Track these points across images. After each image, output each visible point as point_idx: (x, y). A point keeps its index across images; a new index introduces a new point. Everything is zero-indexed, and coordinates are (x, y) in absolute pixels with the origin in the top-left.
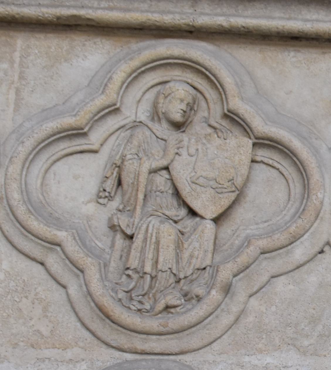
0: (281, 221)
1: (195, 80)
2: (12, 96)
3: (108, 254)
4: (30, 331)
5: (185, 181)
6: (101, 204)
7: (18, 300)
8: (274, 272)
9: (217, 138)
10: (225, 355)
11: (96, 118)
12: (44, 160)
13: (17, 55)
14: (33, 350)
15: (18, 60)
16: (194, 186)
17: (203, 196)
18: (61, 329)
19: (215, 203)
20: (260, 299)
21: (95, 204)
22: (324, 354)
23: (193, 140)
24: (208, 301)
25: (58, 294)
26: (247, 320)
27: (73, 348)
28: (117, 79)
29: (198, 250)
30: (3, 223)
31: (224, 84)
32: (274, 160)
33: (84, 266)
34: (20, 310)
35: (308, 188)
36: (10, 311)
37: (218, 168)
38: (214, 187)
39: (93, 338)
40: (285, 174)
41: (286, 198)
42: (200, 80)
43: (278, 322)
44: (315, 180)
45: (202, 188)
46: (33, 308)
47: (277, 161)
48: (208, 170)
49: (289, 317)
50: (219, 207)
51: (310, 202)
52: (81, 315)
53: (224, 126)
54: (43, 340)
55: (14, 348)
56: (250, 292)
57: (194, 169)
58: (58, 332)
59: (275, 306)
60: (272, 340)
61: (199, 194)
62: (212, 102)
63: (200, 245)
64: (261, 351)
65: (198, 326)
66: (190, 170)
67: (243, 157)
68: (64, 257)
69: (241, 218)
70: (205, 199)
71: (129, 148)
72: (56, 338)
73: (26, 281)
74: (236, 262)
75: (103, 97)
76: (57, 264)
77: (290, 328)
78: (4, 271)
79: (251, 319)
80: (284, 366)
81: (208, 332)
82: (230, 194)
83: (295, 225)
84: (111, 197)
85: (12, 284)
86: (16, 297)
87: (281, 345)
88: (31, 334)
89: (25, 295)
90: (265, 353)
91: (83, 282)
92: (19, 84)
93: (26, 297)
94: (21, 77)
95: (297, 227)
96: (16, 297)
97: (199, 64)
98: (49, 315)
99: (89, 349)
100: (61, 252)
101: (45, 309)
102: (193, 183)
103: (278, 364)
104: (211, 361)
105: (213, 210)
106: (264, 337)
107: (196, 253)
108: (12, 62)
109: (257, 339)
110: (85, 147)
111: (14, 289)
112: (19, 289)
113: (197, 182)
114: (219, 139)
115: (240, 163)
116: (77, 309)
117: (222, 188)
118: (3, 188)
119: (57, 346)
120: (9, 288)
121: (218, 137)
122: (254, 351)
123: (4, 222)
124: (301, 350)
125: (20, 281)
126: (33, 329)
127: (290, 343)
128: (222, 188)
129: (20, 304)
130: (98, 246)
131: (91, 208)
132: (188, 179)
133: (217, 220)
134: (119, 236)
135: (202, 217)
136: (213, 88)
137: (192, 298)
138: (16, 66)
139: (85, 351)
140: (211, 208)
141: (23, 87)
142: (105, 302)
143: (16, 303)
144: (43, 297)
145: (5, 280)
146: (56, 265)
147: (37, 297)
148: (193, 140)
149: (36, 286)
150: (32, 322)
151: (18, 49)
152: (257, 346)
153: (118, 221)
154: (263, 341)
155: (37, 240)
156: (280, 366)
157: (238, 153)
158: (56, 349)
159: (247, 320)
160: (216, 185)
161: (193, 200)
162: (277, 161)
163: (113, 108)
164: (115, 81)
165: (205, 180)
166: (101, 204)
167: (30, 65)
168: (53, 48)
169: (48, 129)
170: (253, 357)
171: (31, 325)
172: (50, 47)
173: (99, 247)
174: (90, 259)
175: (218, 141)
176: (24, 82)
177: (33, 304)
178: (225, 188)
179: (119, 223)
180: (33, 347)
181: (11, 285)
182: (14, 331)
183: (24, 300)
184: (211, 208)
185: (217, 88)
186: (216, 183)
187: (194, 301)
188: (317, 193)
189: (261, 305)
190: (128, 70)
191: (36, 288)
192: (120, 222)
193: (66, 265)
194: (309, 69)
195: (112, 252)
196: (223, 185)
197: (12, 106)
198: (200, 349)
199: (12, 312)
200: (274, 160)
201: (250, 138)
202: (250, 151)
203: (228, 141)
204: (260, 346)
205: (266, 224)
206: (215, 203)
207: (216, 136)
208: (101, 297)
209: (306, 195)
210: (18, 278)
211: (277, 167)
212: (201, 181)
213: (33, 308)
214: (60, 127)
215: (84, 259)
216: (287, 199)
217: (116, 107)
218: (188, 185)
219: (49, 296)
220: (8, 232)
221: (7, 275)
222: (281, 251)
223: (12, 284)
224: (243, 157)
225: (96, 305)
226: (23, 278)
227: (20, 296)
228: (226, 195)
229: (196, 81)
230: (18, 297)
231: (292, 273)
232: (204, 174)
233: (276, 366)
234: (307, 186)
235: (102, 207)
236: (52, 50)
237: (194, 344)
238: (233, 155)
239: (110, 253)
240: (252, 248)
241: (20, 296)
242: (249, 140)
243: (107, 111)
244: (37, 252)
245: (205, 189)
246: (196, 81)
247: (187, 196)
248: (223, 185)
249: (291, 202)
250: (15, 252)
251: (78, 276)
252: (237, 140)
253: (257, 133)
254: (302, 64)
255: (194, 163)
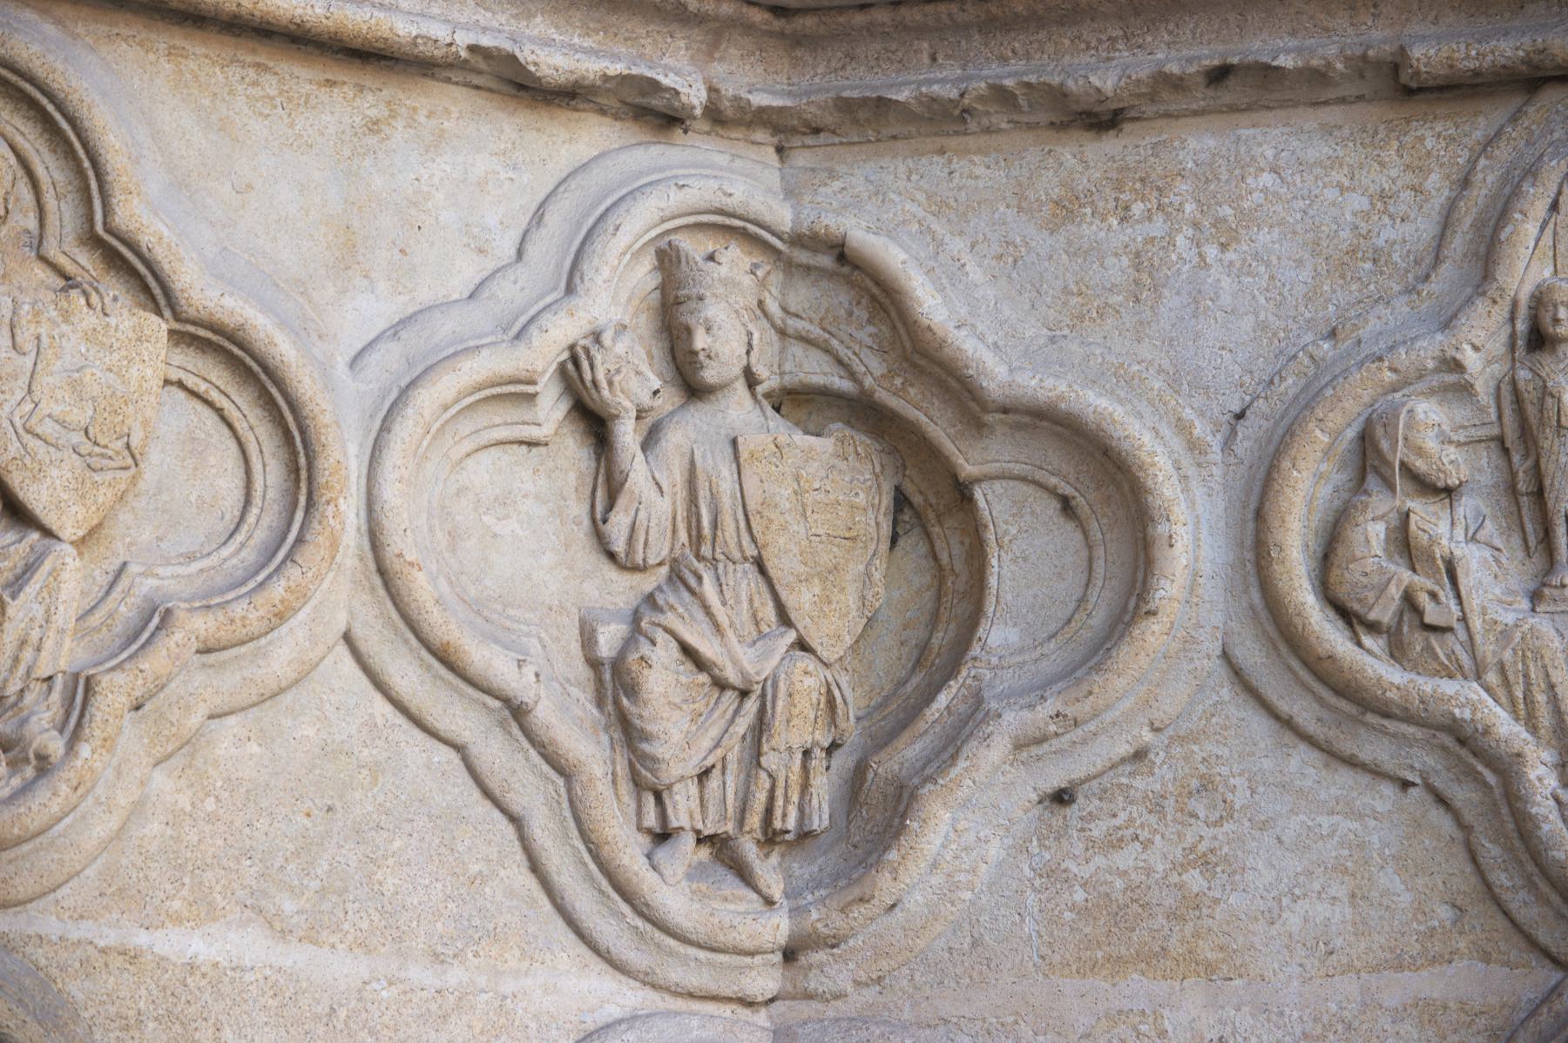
0: (234, 561)
1: (7, 118)
5: (6, 424)
8: (218, 702)
9: (85, 309)
10: (91, 922)
16: (27, 438)
17: (55, 472)
19: (83, 496)
20: (176, 774)
22: (331, 940)
23: (26, 307)
24: (72, 774)
26: (146, 831)
29: (41, 626)
31: (102, 151)
32: (211, 383)
35: (310, 479)
37: (93, 399)
38: (83, 452)
40: (237, 425)
41: (237, 495)
42: (18, 121)
43: (220, 842)
44: (331, 460)
45: (52, 450)
47: (217, 387)
48: (67, 399)
49: (247, 831)
50: (94, 508)
51: (320, 523)
53: (83, 268)
56: (158, 752)
57: (30, 391)
59: (212, 799)
60: (206, 890)
61: (44, 468)
62: (51, 190)
63: (47, 611)
64: (178, 920)
65: (38, 840)
66: (19, 395)
67: (149, 372)
69: (128, 540)
70: (58, 482)
74: (141, 671)
77: (248, 862)
79: (154, 827)
80: (233, 965)
81: (56, 856)
82: (119, 474)
83: (283, 582)
87: (228, 908)
90: (188, 925)
95: (288, 589)
97: (32, 80)
102: (28, 432)
103: (221, 959)
104: (53, 937)
105: (80, 517)
106: (187, 880)
107: (35, 635)
109: (168, 887)
113: (39, 430)
114: (91, 312)
115: (141, 386)
117: (102, 455)
121: (89, 304)
122: (161, 918)
124: (278, 926)
127: (248, 903)
128: (102, 455)
132: (18, 422)
133: (81, 543)
135: (47, 533)
136: (54, 151)
137: (27, 761)
140: (74, 509)
148: (26, 307)
152: (168, 903)
154: (184, 892)
156: (225, 964)
157: (137, 359)
159: (146, 831)
160: (87, 447)
161: (27, 481)
162: (217, 387)
165: (58, 427)
170: (160, 933)
175: (90, 320)
178: (110, 458)
184: (74, 509)
185: (70, 152)
186: (84, 439)
187: (29, 772)
188: (337, 499)
189: (178, 791)
194: (291, 125)
196: (105, 447)
198: (31, 900)
200: (211, 383)
201: (159, 313)
202: (163, 352)
203: (113, 321)
204: (176, 904)
205: (195, 567)
206: (83, 496)
207: (82, 301)
209: (302, 499)
211: (218, 405)
212: (48, 428)
216: (242, 500)
218: (14, 438)
222: (243, 649)
224: (149, 372)
228: (109, 476)
229: (7, 122)
231: (255, 709)
232: (57, 410)
233: (216, 965)
234: (304, 474)
237: (21, 889)
238: (125, 363)
240: (178, 636)
242: (160, 320)
245: (59, 455)
246: (7, 122)
247: (10, 468)
248: (105, 447)
249: (255, 511)
252: (135, 319)
253: (185, 308)
254: (275, 107)
255: (28, 374)
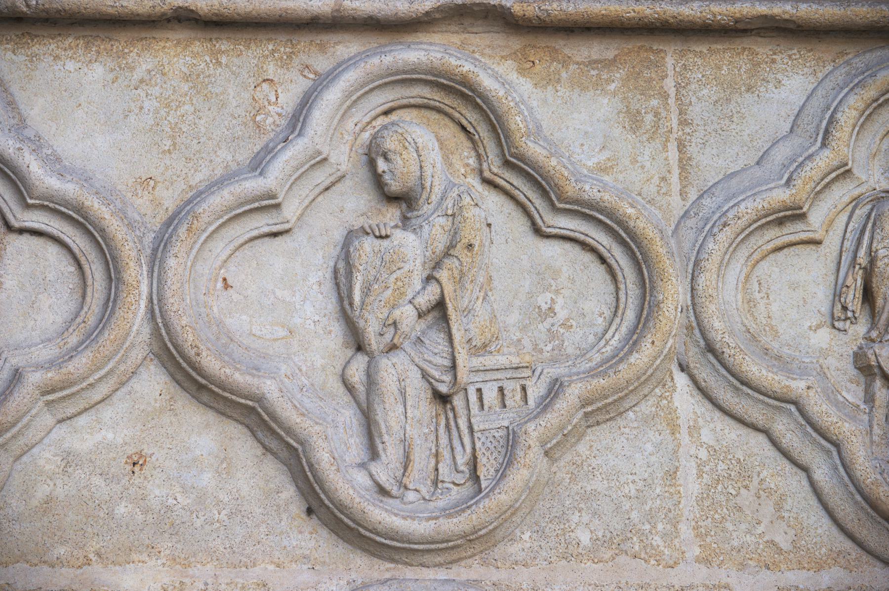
2: (673, 154)
3: (865, 413)
4: (761, 541)
6: (839, 330)
7: (734, 493)
11: (818, 188)
12: (742, 261)
13: (669, 84)
14: (768, 572)
15: (672, 92)
18: (807, 539)
21: (828, 330)
25: (796, 482)
27: (830, 568)
28: (845, 122)
30: (696, 367)
33: (841, 437)
34: (740, 509)
36: (725, 510)
39: (859, 550)
46: (760, 504)
52: (840, 515)
54: (782, 557)
55: (739, 570)
58: (803, 542)
68: (803, 423)
71: (879, 237)
72: (802, 553)
73: (742, 460)
75: (826, 152)
76: (791, 432)
78: (705, 446)
84: (856, 318)
85: (722, 466)
86: (730, 487)
88: (761, 546)
89: (744, 484)
91: (838, 462)
92: (680, 133)
93: (746, 487)
94: (684, 123)
96: (730, 487)
98: (786, 515)
99: (856, 570)
100: (797, 413)
101: (779, 507)
108: (665, 96)
110: (804, 236)
111: (726, 475)
112: (733, 474)
116: (831, 504)
118: (692, 311)
119: (806, 565)
120: (717, 473)
123: (698, 365)
125: (733, 462)
126: (765, 539)
129: (738, 498)
130: (847, 400)
131: (823, 337)
134: (878, 383)
138: (672, 101)
139: (851, 572)
141: (688, 137)
142: (882, 494)
143: (731, 497)
144: (772, 486)
145: (709, 460)
146: (788, 435)
147: (763, 487)
149: (758, 469)
150: (760, 529)
151: (671, 73)
153: (877, 360)
155: (756, 395)
158: (805, 571)
163: (842, 170)
164: (843, 124)
166: (839, 330)
167: (694, 99)
168: (725, 68)
169: (749, 211)
171: (761, 532)
172: (719, 68)
173: (850, 403)
174: (847, 425)
176: (687, 130)
177: (759, 498)
179: (878, 362)
180: (769, 569)
181: (719, 468)
182: (735, 543)
183: (743, 491)
190: (861, 105)
191: (759, 473)
192: (880, 360)
193: (806, 434)
195: (871, 410)
197: (676, 171)
199: (727, 512)
208: (874, 487)
210: (729, 457)
213: (760, 504)
214: (769, 207)
215: (838, 425)
217: (847, 168)
219: (781, 484)
220: (705, 382)
221: (712, 453)
223: (722, 466)
225: (866, 498)
226: (736, 456)
227: (735, 485)
230: (734, 488)
235: (841, 335)
236: (723, 72)
239: (867, 411)
241: (735, 485)
243: (833, 175)
244: (756, 414)
250: (717, 414)
251: (828, 452)
